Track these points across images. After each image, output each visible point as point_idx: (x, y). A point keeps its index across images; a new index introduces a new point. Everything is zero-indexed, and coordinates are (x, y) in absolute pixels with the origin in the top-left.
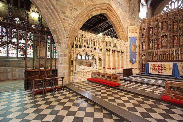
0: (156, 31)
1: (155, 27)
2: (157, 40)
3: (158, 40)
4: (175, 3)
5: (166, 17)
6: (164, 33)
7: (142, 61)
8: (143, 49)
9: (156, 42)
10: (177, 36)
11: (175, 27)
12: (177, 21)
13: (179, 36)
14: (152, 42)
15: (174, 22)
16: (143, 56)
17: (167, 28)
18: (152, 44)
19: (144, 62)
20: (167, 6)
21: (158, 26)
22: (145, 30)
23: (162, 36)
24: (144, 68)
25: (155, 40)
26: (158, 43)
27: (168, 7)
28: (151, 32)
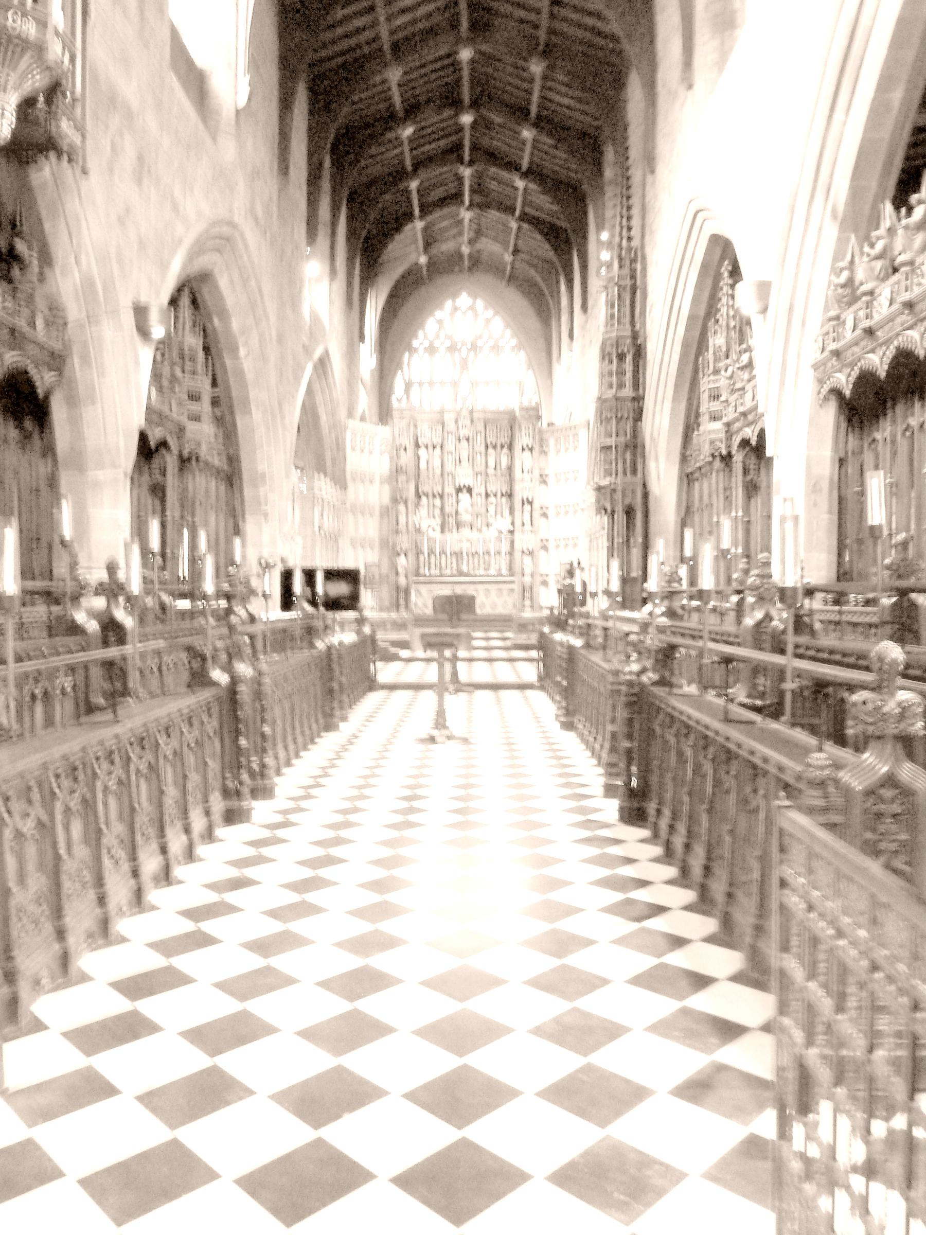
0: (437, 463)
1: (434, 447)
2: (441, 496)
3: (446, 496)
4: (464, 313)
5: (468, 422)
6: (465, 477)
7: (397, 574)
8: (397, 524)
9: (438, 502)
10: (495, 495)
11: (491, 464)
12: (495, 447)
13: (499, 495)
14: (424, 499)
15: (487, 447)
16: (398, 554)
17: (471, 460)
18: (426, 508)
19: (402, 581)
20: (438, 314)
21: (446, 448)
22: (405, 450)
23: (457, 486)
24: (402, 602)
25: (434, 496)
26: (448, 509)
27: (440, 322)
28: (423, 465)
